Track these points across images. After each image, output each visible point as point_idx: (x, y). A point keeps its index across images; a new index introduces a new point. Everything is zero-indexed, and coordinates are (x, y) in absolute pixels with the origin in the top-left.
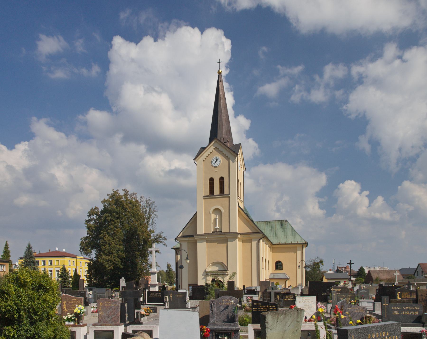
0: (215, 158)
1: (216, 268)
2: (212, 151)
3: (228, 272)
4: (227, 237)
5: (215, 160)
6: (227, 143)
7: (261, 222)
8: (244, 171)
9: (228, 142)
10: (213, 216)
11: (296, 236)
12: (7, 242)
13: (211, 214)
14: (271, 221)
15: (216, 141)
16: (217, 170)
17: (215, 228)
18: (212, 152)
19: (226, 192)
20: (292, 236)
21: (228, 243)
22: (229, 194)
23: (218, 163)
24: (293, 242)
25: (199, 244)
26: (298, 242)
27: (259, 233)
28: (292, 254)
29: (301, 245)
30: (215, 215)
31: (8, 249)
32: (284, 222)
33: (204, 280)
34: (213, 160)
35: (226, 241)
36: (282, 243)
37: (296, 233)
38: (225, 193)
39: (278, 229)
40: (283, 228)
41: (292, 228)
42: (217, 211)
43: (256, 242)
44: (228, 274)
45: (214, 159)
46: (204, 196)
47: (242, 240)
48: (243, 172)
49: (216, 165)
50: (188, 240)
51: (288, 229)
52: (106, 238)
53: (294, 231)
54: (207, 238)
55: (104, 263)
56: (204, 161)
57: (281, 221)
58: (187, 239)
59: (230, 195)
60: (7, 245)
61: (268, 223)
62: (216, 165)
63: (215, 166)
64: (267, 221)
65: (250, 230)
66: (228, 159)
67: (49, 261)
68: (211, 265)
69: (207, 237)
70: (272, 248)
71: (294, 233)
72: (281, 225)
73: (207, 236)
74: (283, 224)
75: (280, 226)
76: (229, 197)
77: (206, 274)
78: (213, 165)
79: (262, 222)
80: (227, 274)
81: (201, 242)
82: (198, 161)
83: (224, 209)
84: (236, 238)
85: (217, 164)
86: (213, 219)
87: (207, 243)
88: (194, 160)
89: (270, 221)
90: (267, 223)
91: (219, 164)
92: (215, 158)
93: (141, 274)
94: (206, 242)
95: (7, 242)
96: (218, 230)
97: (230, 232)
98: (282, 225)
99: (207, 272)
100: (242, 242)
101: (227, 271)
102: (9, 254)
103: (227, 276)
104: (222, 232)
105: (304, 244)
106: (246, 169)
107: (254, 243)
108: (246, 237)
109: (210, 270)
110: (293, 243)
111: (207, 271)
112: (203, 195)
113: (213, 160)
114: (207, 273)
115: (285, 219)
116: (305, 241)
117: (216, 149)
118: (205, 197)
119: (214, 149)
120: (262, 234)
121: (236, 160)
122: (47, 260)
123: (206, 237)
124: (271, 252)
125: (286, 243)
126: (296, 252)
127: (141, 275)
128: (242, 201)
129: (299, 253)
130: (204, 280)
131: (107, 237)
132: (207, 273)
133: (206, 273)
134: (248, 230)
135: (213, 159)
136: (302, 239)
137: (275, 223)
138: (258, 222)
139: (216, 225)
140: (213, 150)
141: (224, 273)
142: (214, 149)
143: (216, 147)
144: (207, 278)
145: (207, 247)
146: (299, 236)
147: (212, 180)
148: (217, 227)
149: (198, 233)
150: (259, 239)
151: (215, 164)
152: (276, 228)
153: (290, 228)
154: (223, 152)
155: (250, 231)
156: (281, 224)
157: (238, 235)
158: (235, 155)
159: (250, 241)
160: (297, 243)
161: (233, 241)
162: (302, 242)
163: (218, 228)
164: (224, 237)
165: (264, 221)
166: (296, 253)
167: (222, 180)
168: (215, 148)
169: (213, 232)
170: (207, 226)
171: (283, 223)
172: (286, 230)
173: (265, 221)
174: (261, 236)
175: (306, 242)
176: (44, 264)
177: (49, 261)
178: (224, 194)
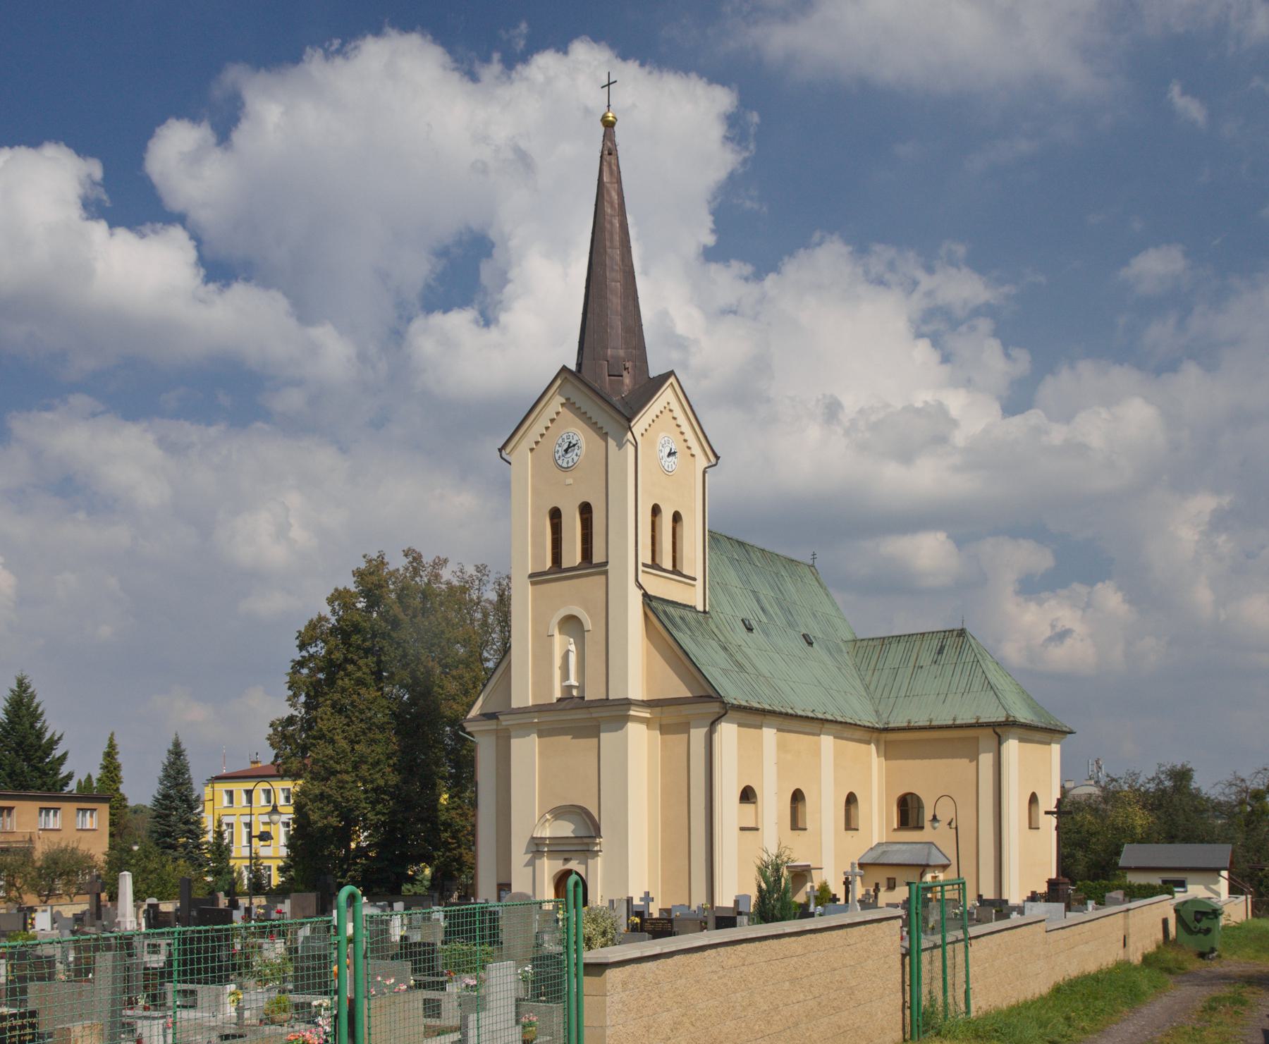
0: (564, 436)
1: (566, 829)
2: (558, 413)
3: (600, 844)
4: (594, 715)
5: (566, 446)
6: (622, 376)
7: (869, 639)
8: (706, 468)
9: (625, 373)
10: (561, 643)
11: (983, 693)
12: (112, 734)
13: (553, 635)
14: (905, 636)
15: (566, 378)
16: (570, 481)
17: (564, 684)
18: (555, 417)
19: (597, 558)
20: (965, 696)
21: (603, 735)
22: (607, 562)
23: (574, 456)
24: (960, 717)
25: (516, 743)
26: (978, 718)
27: (710, 697)
28: (961, 765)
29: (990, 731)
30: (565, 637)
31: (113, 758)
32: (953, 639)
33: (531, 868)
34: (560, 446)
35: (592, 730)
36: (916, 724)
37: (987, 682)
38: (596, 560)
39: (922, 667)
40: (942, 663)
41: (975, 663)
42: (571, 624)
43: (704, 730)
44: (601, 851)
45: (563, 440)
46: (531, 576)
47: (658, 726)
48: (704, 472)
49: (568, 462)
50: (497, 731)
51: (962, 665)
52: (325, 722)
53: (980, 673)
54: (536, 720)
55: (306, 804)
56: (532, 450)
57: (943, 634)
58: (491, 725)
59: (608, 567)
60: (112, 746)
61: (894, 646)
62: (568, 462)
63: (565, 465)
64: (889, 637)
65: (686, 690)
66: (604, 436)
67: (283, 790)
68: (548, 816)
69: (538, 718)
70: (885, 742)
71: (977, 685)
72: (940, 650)
73: (536, 714)
74: (947, 648)
75: (933, 653)
76: (606, 573)
77: (535, 850)
78: (560, 462)
79: (873, 639)
80: (596, 848)
81: (524, 737)
82: (516, 453)
83: (591, 617)
84: (626, 719)
85: (570, 460)
86: (563, 652)
87: (539, 737)
88: (500, 450)
89: (900, 636)
90: (890, 644)
91: (576, 458)
92: (564, 436)
93: (450, 840)
94: (536, 735)
95: (112, 734)
96: (575, 693)
97: (607, 699)
98: (940, 651)
99: (536, 841)
100: (658, 732)
101: (595, 837)
102: (116, 776)
103: (598, 856)
104: (586, 699)
105: (1000, 724)
106: (717, 458)
107: (698, 734)
108: (670, 715)
109: (548, 835)
110: (958, 722)
111: (536, 838)
112: (530, 572)
113: (560, 446)
114: (537, 844)
115: (958, 626)
116: (1008, 716)
117: (568, 404)
118: (537, 578)
119: (562, 405)
120: (718, 704)
121: (628, 440)
122: (239, 788)
123: (535, 718)
124: (878, 757)
125: (934, 723)
126: (974, 757)
127: (453, 846)
128: (694, 579)
129: (986, 759)
130: (531, 868)
131: (329, 720)
132: (537, 844)
133: (537, 847)
134: (678, 688)
135: (560, 441)
136: (1001, 706)
137: (918, 644)
138: (858, 643)
139: (565, 675)
140: (560, 410)
141: (587, 844)
142: (562, 405)
143: (568, 399)
144: (537, 862)
145: (540, 753)
146: (992, 692)
147: (555, 515)
148: (573, 681)
149: (515, 705)
150: (710, 721)
151: (566, 460)
152: (917, 665)
153: (967, 660)
154: (588, 415)
155: (684, 692)
156: (940, 644)
157: (629, 710)
158: (626, 424)
159: (684, 728)
160: (974, 721)
161: (616, 731)
162: (994, 720)
163: (571, 687)
164: (585, 716)
165: (880, 638)
166: (975, 762)
167: (586, 510)
168: (564, 401)
169: (559, 700)
170: (543, 679)
171: (948, 644)
172: (949, 668)
173: (884, 638)
174: (717, 710)
175: (1011, 719)
176: (250, 801)
177: (283, 790)
178: (591, 562)
